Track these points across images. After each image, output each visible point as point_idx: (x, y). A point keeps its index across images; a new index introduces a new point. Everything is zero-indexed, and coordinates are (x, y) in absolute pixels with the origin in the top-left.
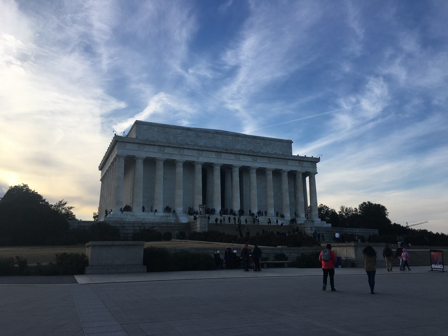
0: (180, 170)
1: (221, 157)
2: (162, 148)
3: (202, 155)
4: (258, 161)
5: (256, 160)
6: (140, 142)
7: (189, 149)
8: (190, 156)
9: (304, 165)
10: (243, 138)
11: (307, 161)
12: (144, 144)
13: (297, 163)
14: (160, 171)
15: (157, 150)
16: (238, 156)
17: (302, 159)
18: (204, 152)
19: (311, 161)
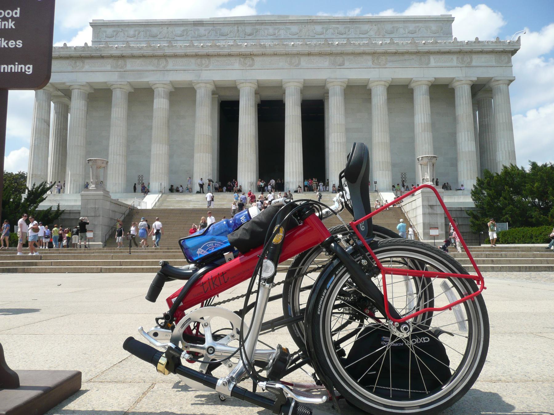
0: (160, 104)
1: (251, 65)
2: (121, 62)
3: (207, 66)
4: (347, 64)
5: (344, 64)
6: (73, 53)
7: (175, 56)
8: (182, 73)
9: (474, 63)
10: (325, 26)
11: (482, 52)
12: (81, 58)
13: (454, 60)
14: (118, 111)
15: (109, 68)
16: (295, 60)
17: (468, 48)
18: (213, 60)
19: (492, 52)
